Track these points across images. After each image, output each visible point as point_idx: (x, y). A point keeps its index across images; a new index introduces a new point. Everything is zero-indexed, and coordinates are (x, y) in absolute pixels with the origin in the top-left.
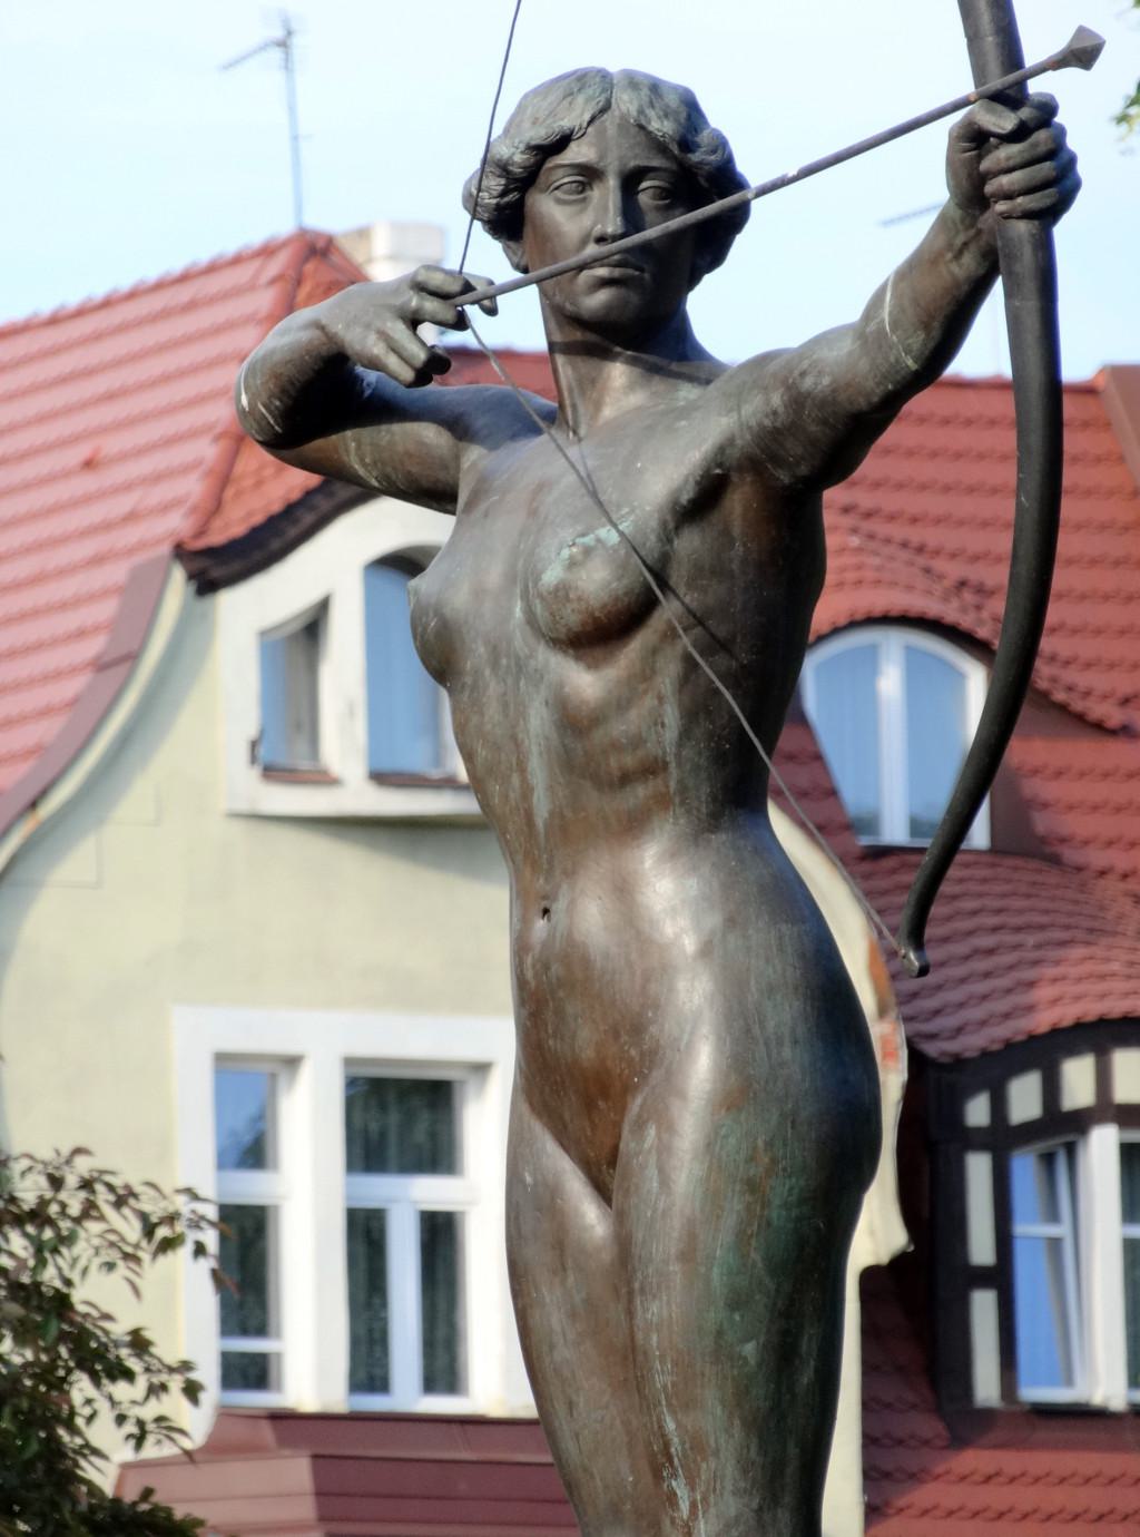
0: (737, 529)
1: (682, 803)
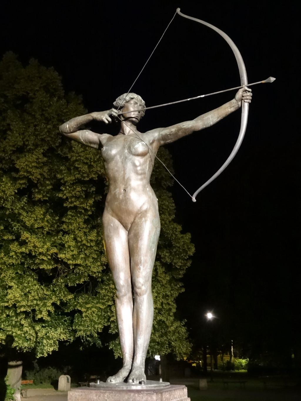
0: (154, 147)
1: (147, 179)
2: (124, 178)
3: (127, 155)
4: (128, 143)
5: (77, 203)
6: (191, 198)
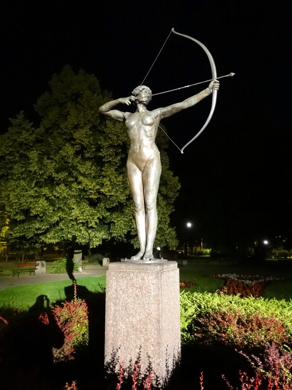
2: (139, 139)
3: (141, 125)
4: (142, 117)
5: (111, 159)
6: (180, 151)
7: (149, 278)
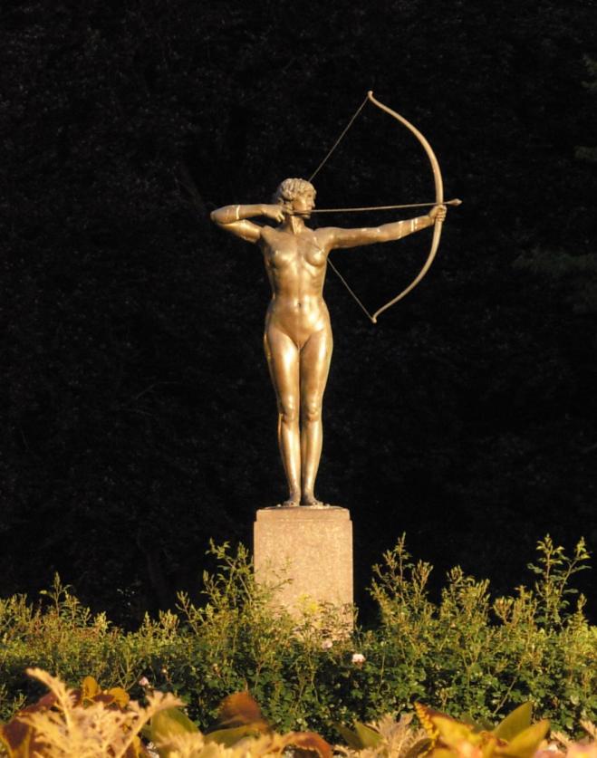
2: (299, 290)
7: (333, 530)
